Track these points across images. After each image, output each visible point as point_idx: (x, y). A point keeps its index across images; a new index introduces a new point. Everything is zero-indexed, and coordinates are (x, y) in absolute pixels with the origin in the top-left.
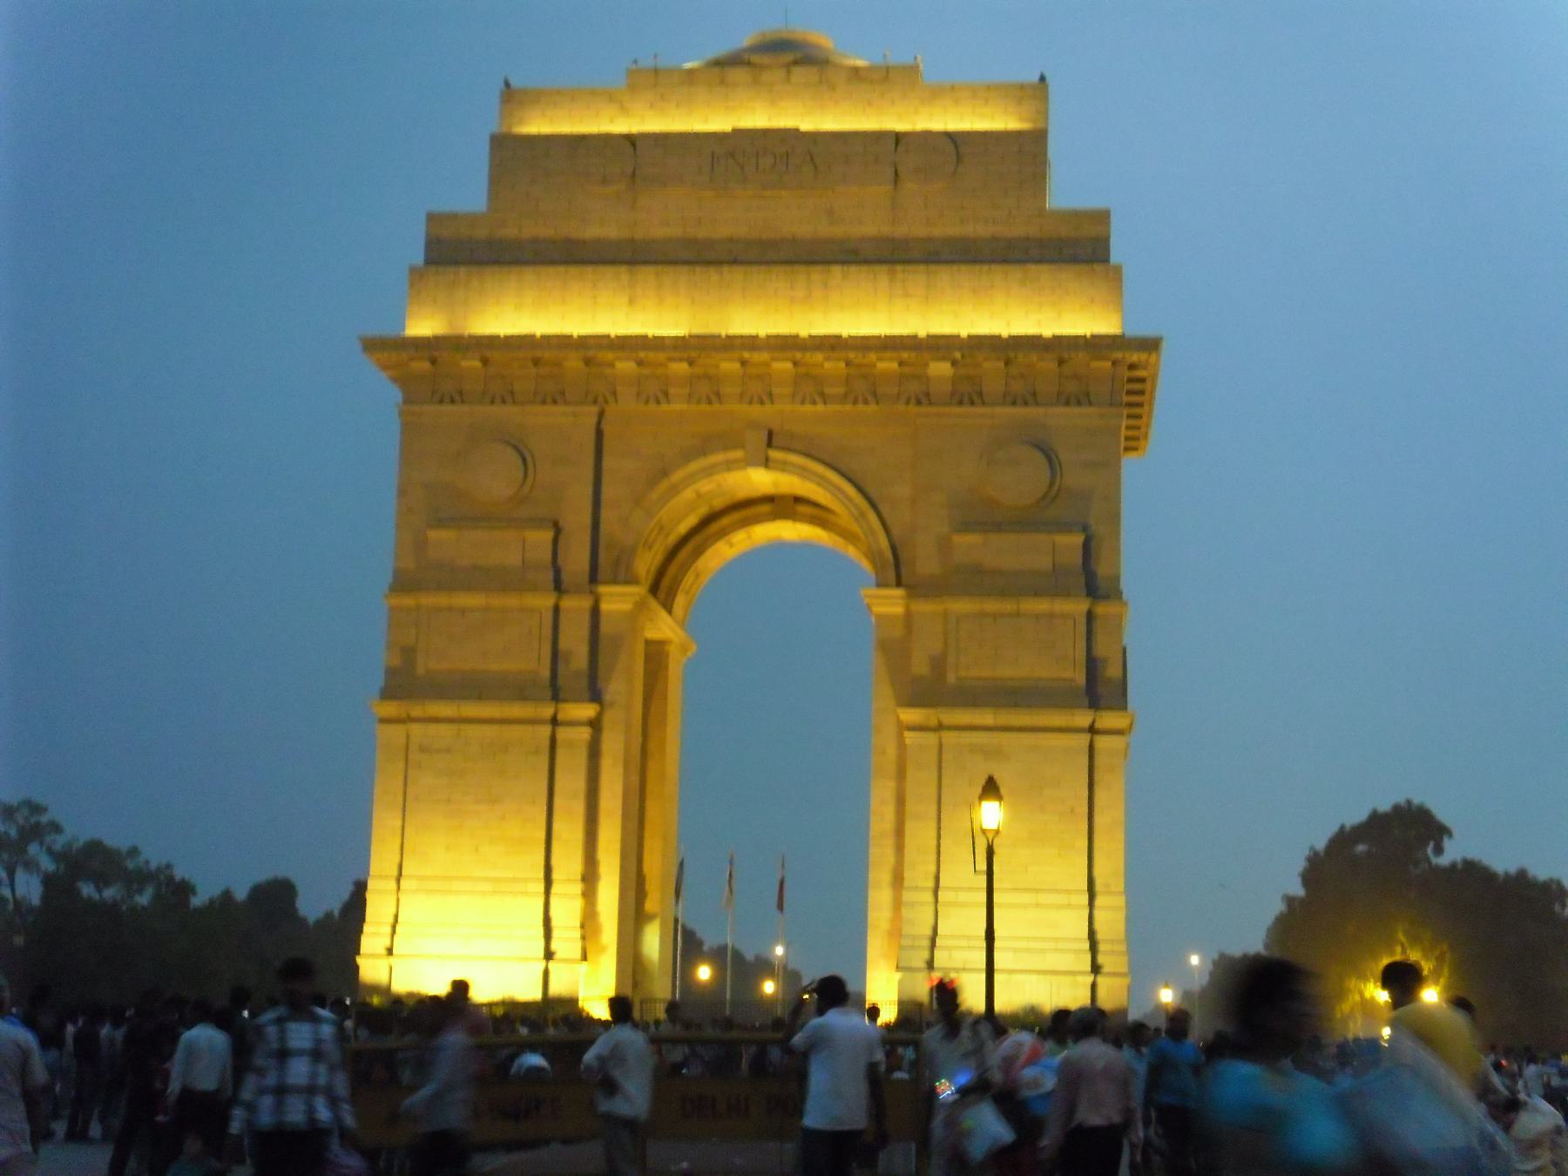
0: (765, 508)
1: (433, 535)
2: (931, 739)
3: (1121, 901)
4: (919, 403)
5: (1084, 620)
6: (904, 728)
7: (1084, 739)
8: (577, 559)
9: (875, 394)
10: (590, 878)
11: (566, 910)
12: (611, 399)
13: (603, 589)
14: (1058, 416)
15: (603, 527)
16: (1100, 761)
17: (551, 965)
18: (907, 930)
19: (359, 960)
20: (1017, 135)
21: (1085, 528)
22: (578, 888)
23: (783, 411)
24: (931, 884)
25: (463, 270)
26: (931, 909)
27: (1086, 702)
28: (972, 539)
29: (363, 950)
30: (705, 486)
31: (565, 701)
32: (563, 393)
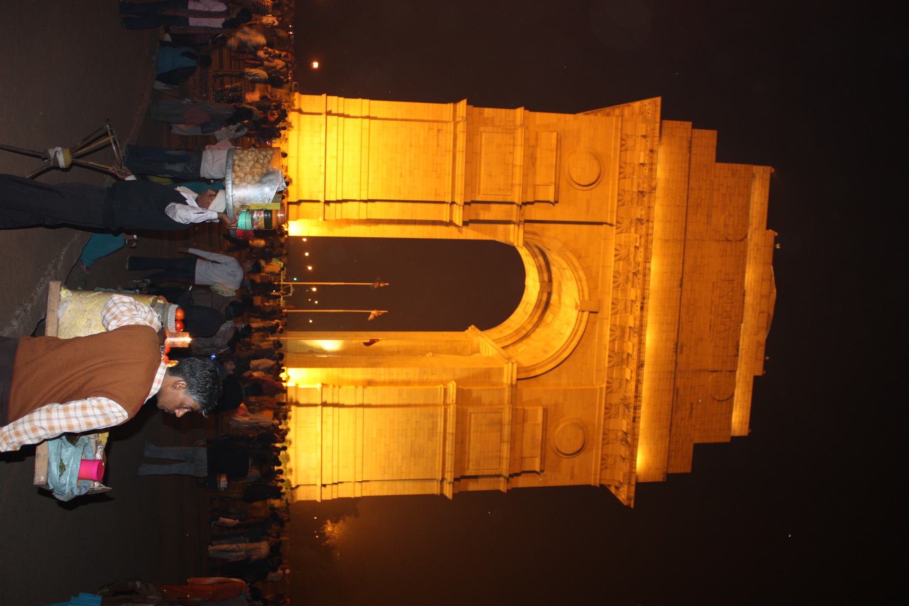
1: (555, 135)
2: (440, 400)
3: (358, 495)
4: (607, 388)
5: (498, 473)
6: (445, 383)
8: (535, 213)
9: (613, 366)
11: (352, 211)
13: (521, 226)
16: (428, 484)
17: (321, 205)
19: (324, 95)
21: (542, 471)
22: (363, 217)
24: (366, 402)
27: (458, 477)
28: (540, 419)
29: (329, 97)
30: (569, 273)
32: (623, 205)
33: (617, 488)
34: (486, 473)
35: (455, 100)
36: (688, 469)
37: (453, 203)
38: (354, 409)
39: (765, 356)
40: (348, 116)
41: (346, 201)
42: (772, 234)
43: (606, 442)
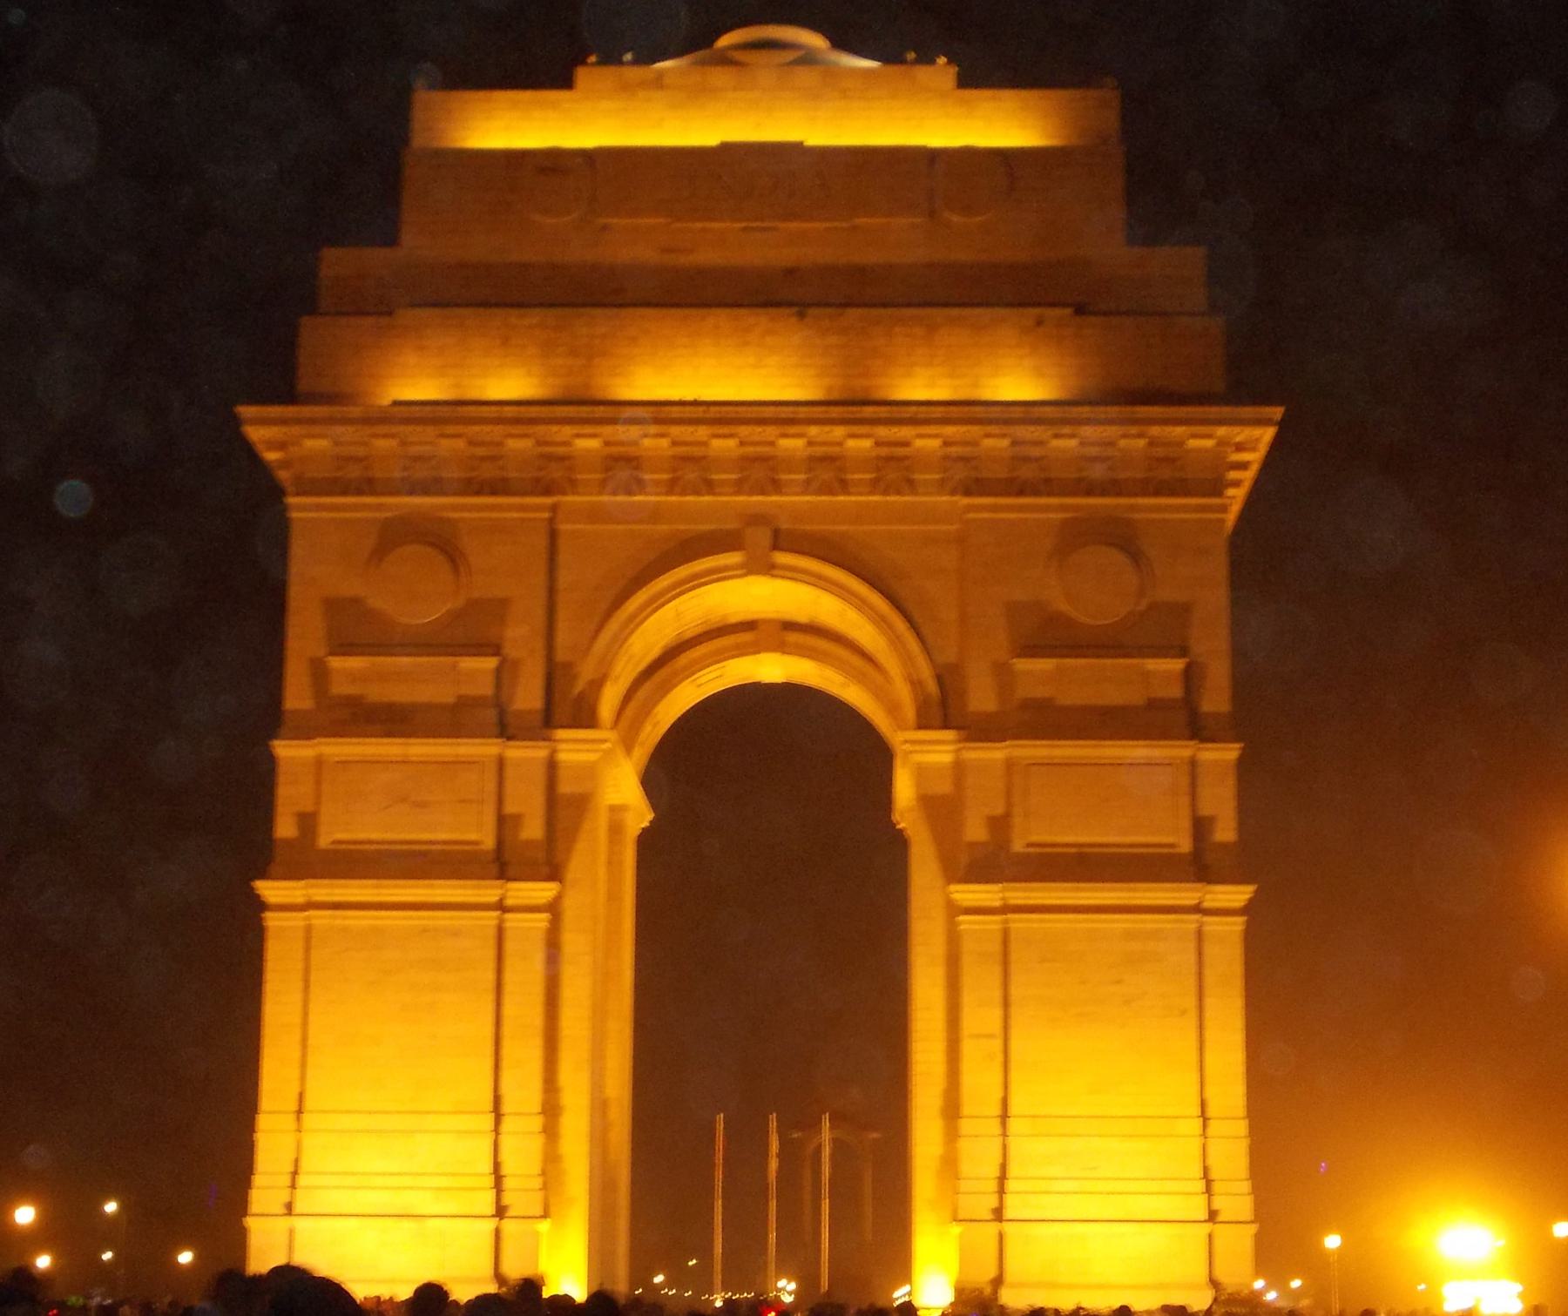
0: (747, 637)
1: (336, 663)
2: (993, 923)
3: (1242, 1127)
8: (528, 696)
10: (551, 1110)
11: (522, 1154)
13: (561, 734)
15: (561, 655)
16: (1210, 950)
17: (508, 1226)
18: (966, 1168)
19: (250, 1222)
21: (1183, 652)
22: (537, 1123)
23: (791, 502)
24: (996, 1110)
25: (369, 321)
26: (996, 1144)
28: (1045, 665)
33: (1240, 448)
34: (1185, 801)
35: (261, 906)
36: (1201, 251)
38: (1012, 1141)
39: (903, 62)
40: (297, 1162)
41: (497, 1166)
42: (582, 75)
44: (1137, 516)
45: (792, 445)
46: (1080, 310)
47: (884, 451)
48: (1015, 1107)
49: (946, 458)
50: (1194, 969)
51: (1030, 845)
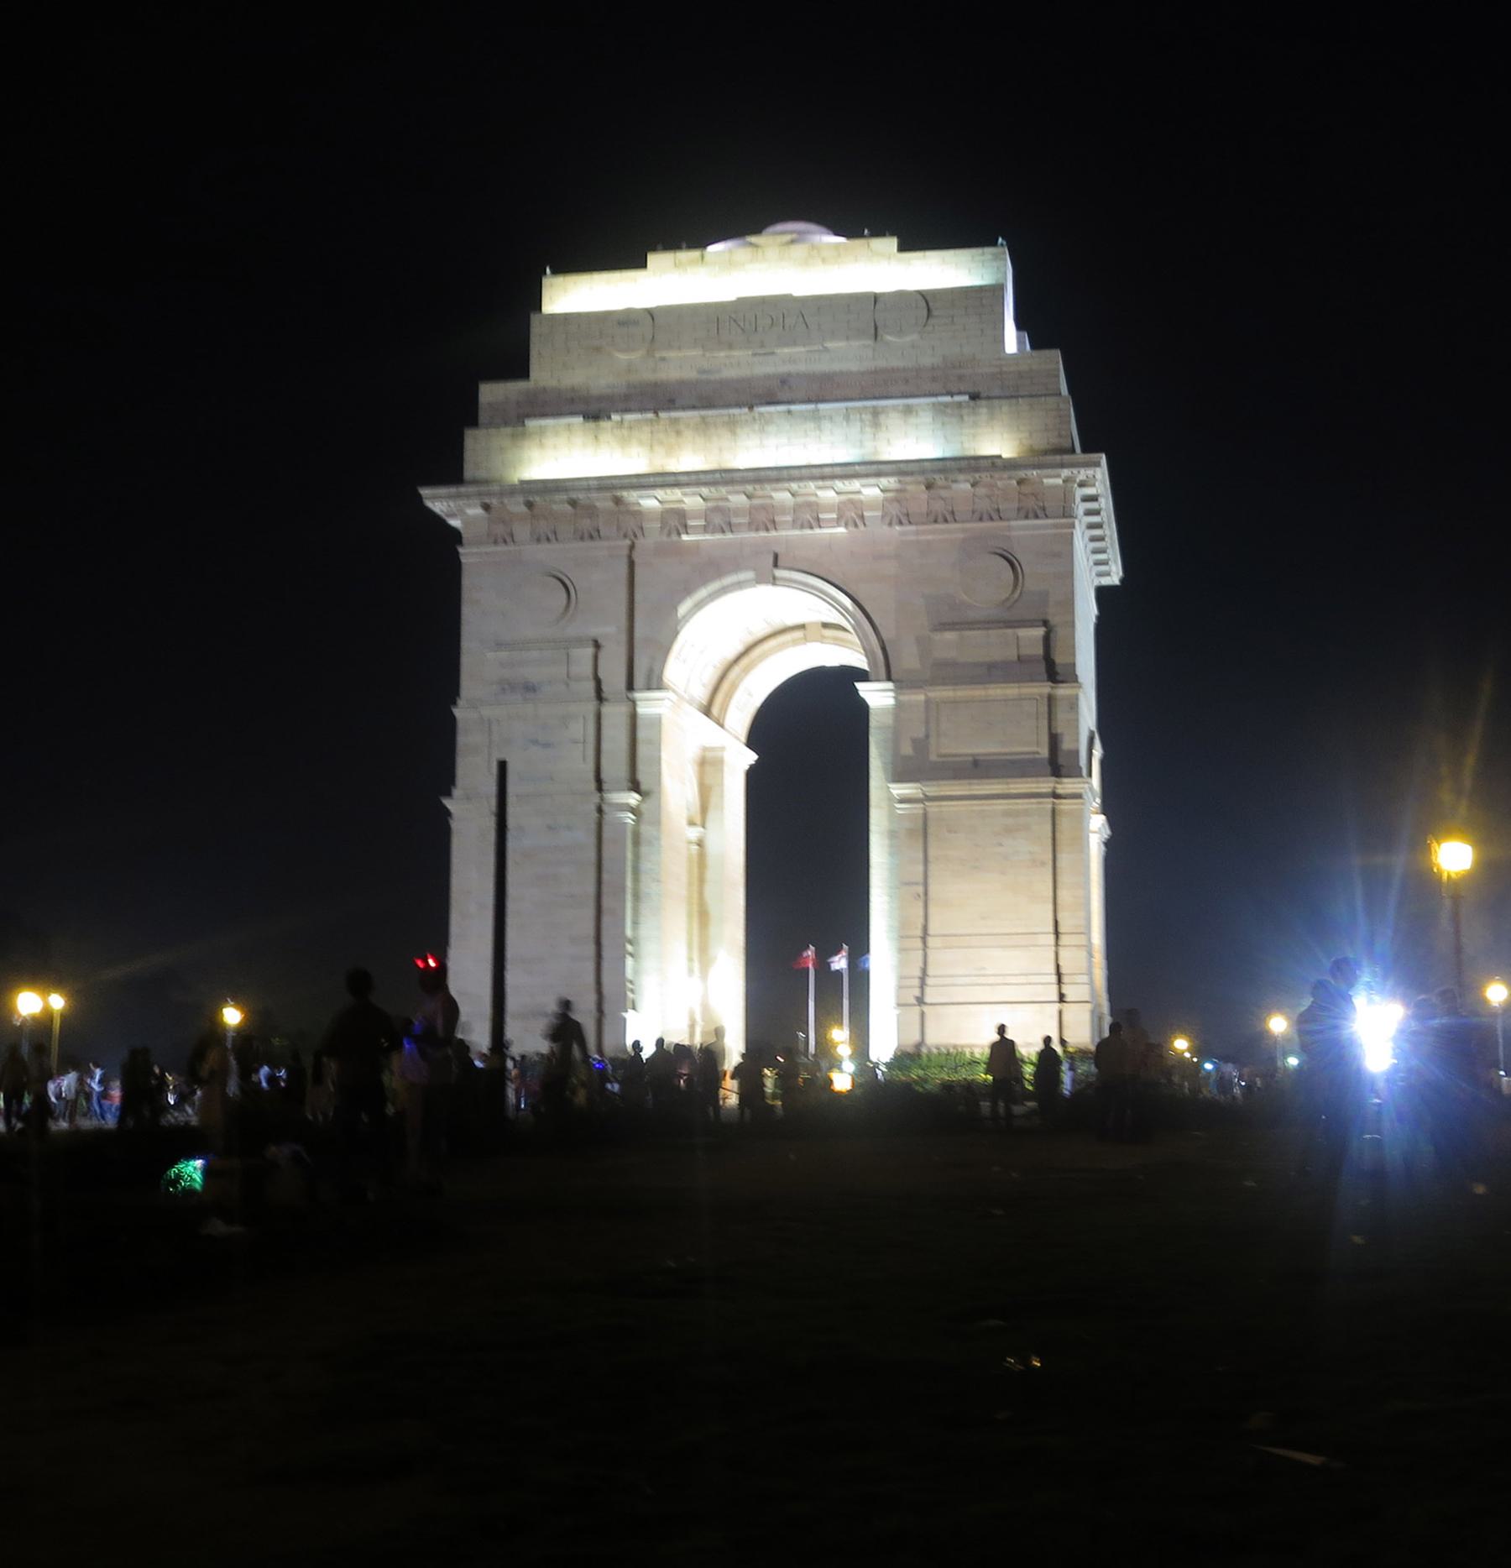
4: (901, 523)
7: (1048, 803)
12: (639, 534)
13: (638, 695)
14: (1021, 529)
20: (980, 289)
21: (1045, 623)
24: (919, 932)
25: (508, 430)
27: (1049, 769)
28: (950, 636)
31: (609, 791)
34: (1046, 722)
35: (448, 813)
37: (600, 810)
38: (929, 952)
42: (653, 259)
43: (997, 515)
44: (1014, 533)
45: (782, 496)
46: (974, 397)
47: (843, 498)
48: (932, 930)
49: (885, 499)
50: (1050, 834)
51: (940, 756)
